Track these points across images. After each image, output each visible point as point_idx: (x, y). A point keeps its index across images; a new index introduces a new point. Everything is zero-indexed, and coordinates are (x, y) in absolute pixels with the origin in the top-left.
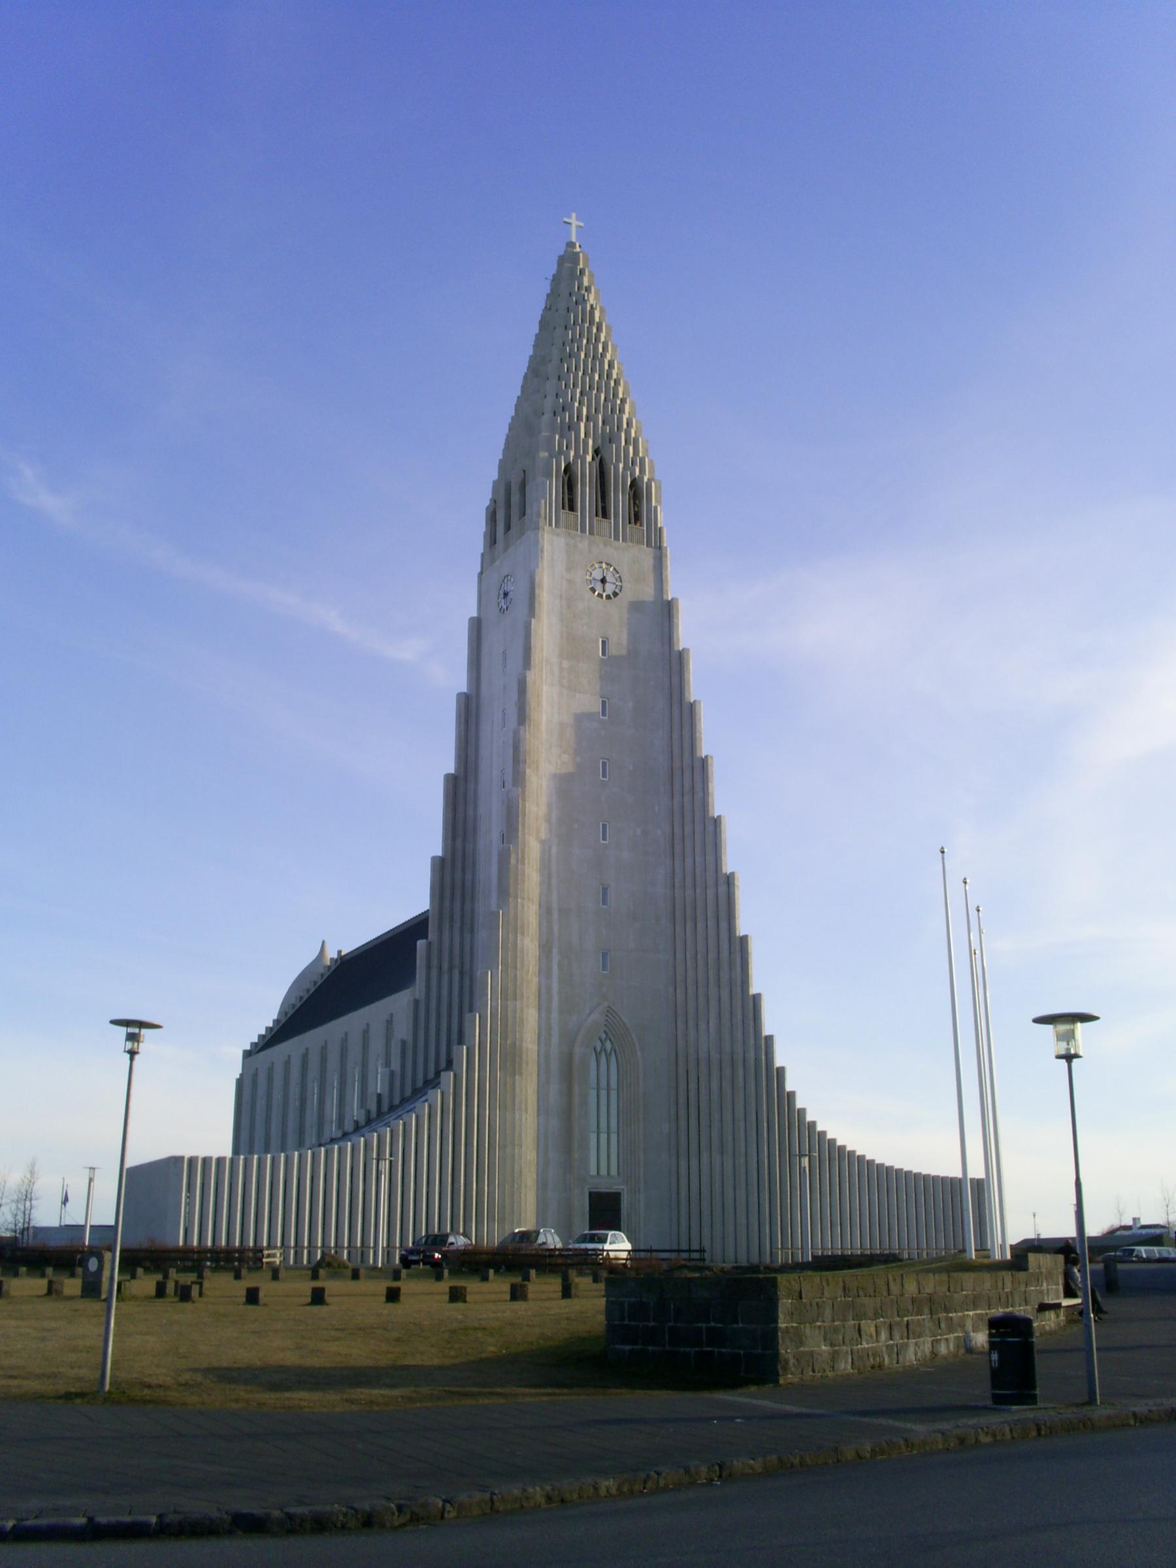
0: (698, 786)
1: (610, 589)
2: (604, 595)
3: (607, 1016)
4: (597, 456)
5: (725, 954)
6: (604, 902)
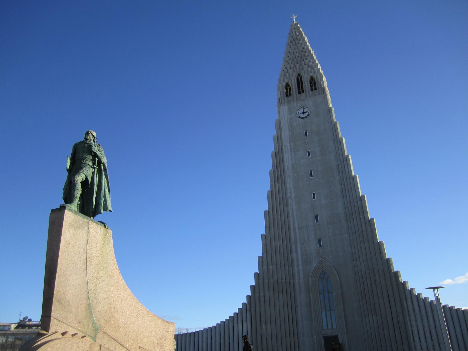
0: (346, 167)
1: (306, 115)
4: (299, 76)
5: (364, 228)
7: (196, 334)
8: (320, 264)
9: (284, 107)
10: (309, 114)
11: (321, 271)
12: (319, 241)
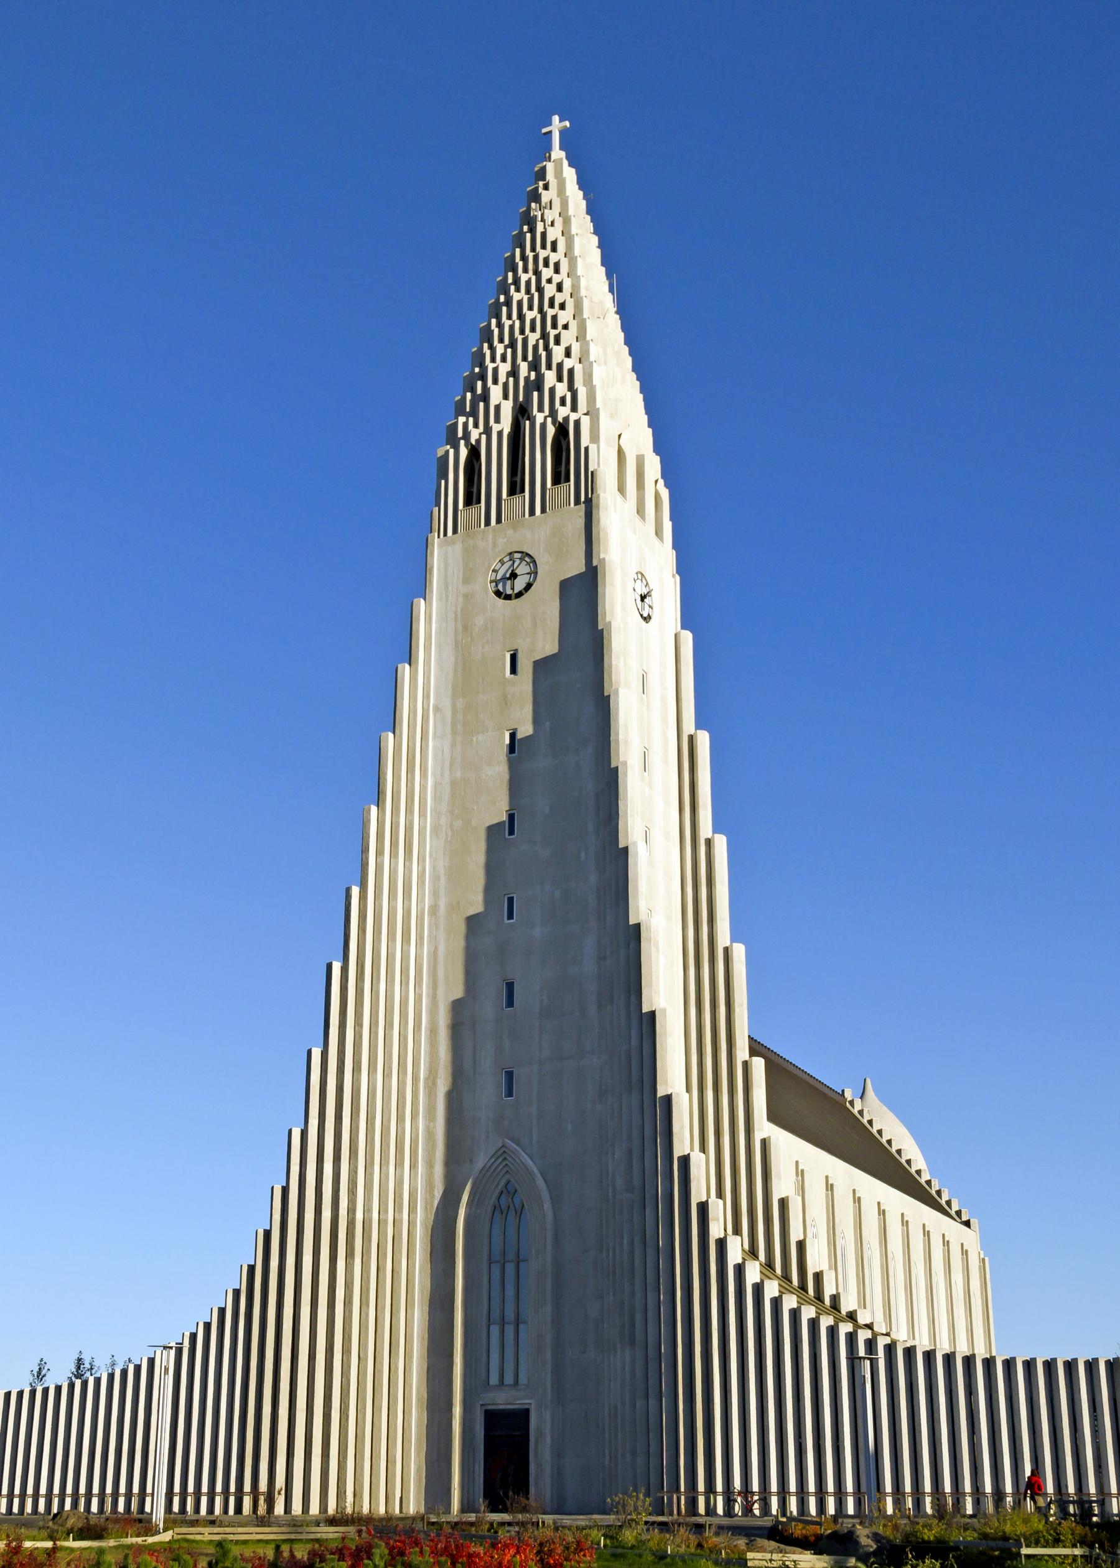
1: (520, 584)
2: (513, 596)
3: (505, 1159)
4: (523, 417)
5: (634, 1042)
6: (510, 1003)
8: (500, 1160)
9: (450, 549)
11: (503, 1183)
12: (510, 1075)
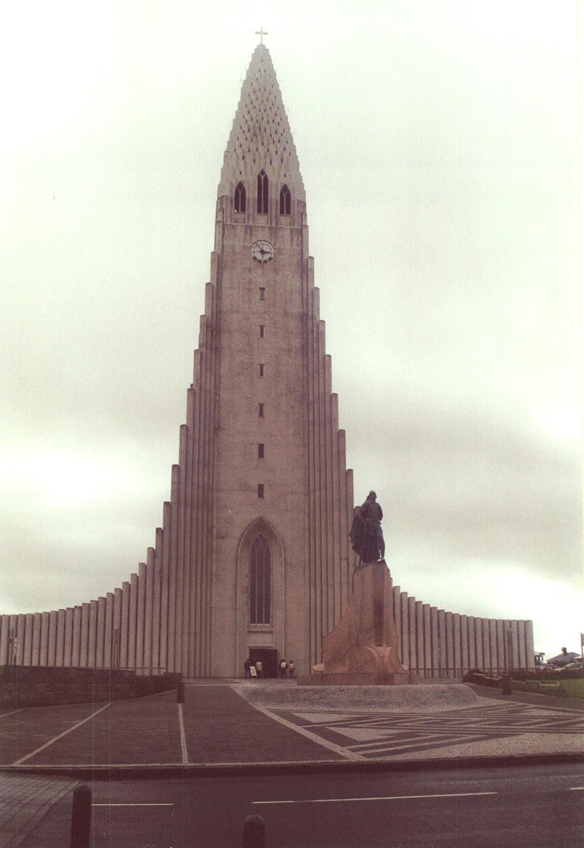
1: (266, 257)
2: (262, 262)
4: (262, 175)
7: (37, 619)
10: (272, 256)
